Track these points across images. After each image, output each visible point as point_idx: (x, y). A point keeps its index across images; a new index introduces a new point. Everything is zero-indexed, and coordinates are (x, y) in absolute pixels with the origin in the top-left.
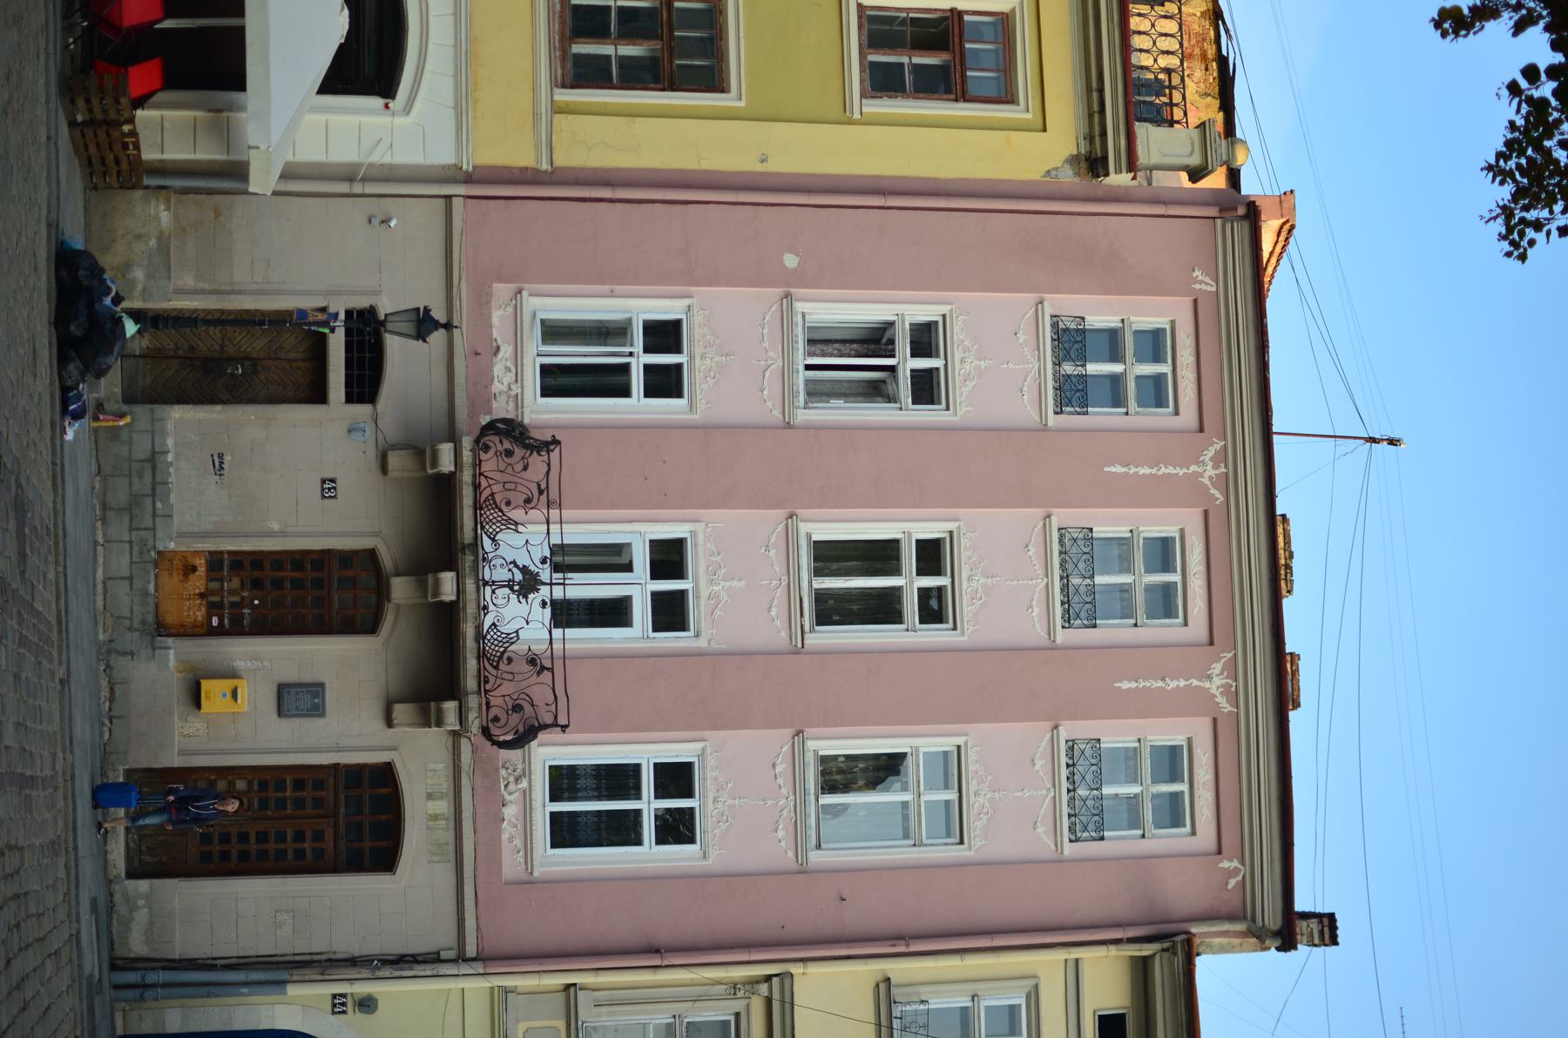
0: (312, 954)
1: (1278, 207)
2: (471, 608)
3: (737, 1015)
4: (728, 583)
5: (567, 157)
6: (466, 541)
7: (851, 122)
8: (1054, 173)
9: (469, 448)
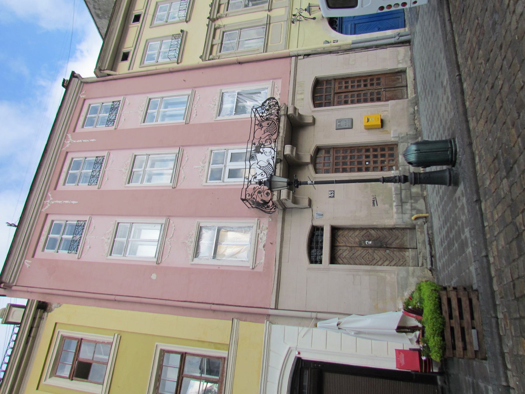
0: (344, 54)
2: (280, 140)
3: (220, 52)
4: (199, 167)
6: (279, 164)
8: (59, 306)
9: (274, 196)
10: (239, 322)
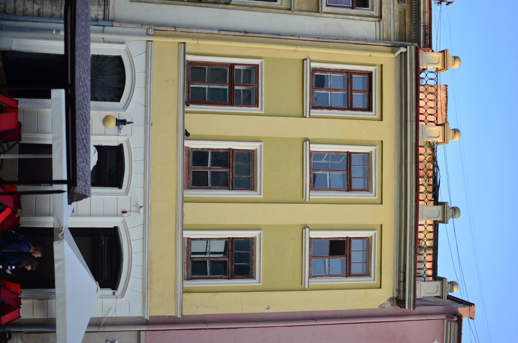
1: (468, 312)
5: (189, 311)
7: (304, 290)
10: (176, 315)
